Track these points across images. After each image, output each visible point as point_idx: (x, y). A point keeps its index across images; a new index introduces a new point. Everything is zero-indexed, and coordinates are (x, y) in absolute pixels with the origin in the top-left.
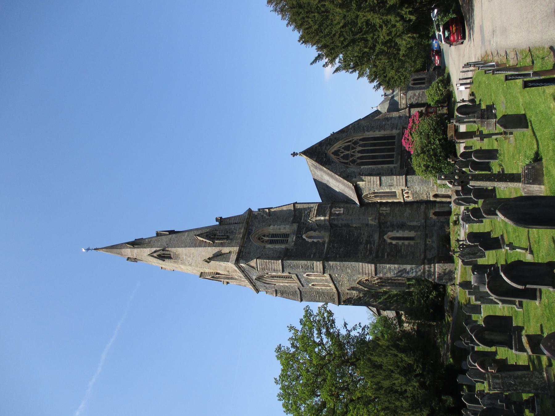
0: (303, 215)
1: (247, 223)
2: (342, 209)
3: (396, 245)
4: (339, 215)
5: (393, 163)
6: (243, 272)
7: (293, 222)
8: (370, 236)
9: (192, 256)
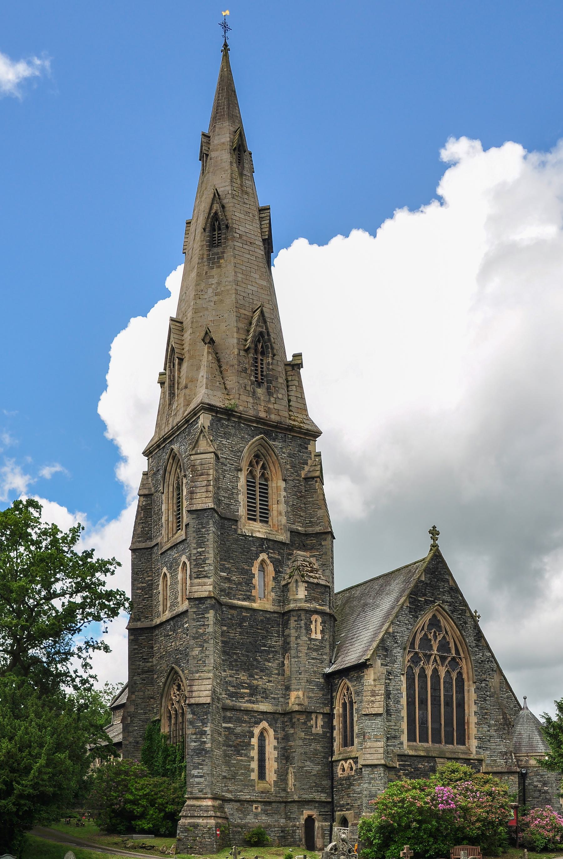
0: (308, 554)
1: (291, 429)
2: (319, 636)
3: (249, 744)
4: (308, 630)
5: (409, 740)
6: (187, 421)
7: (293, 533)
8: (266, 695)
9: (216, 298)
